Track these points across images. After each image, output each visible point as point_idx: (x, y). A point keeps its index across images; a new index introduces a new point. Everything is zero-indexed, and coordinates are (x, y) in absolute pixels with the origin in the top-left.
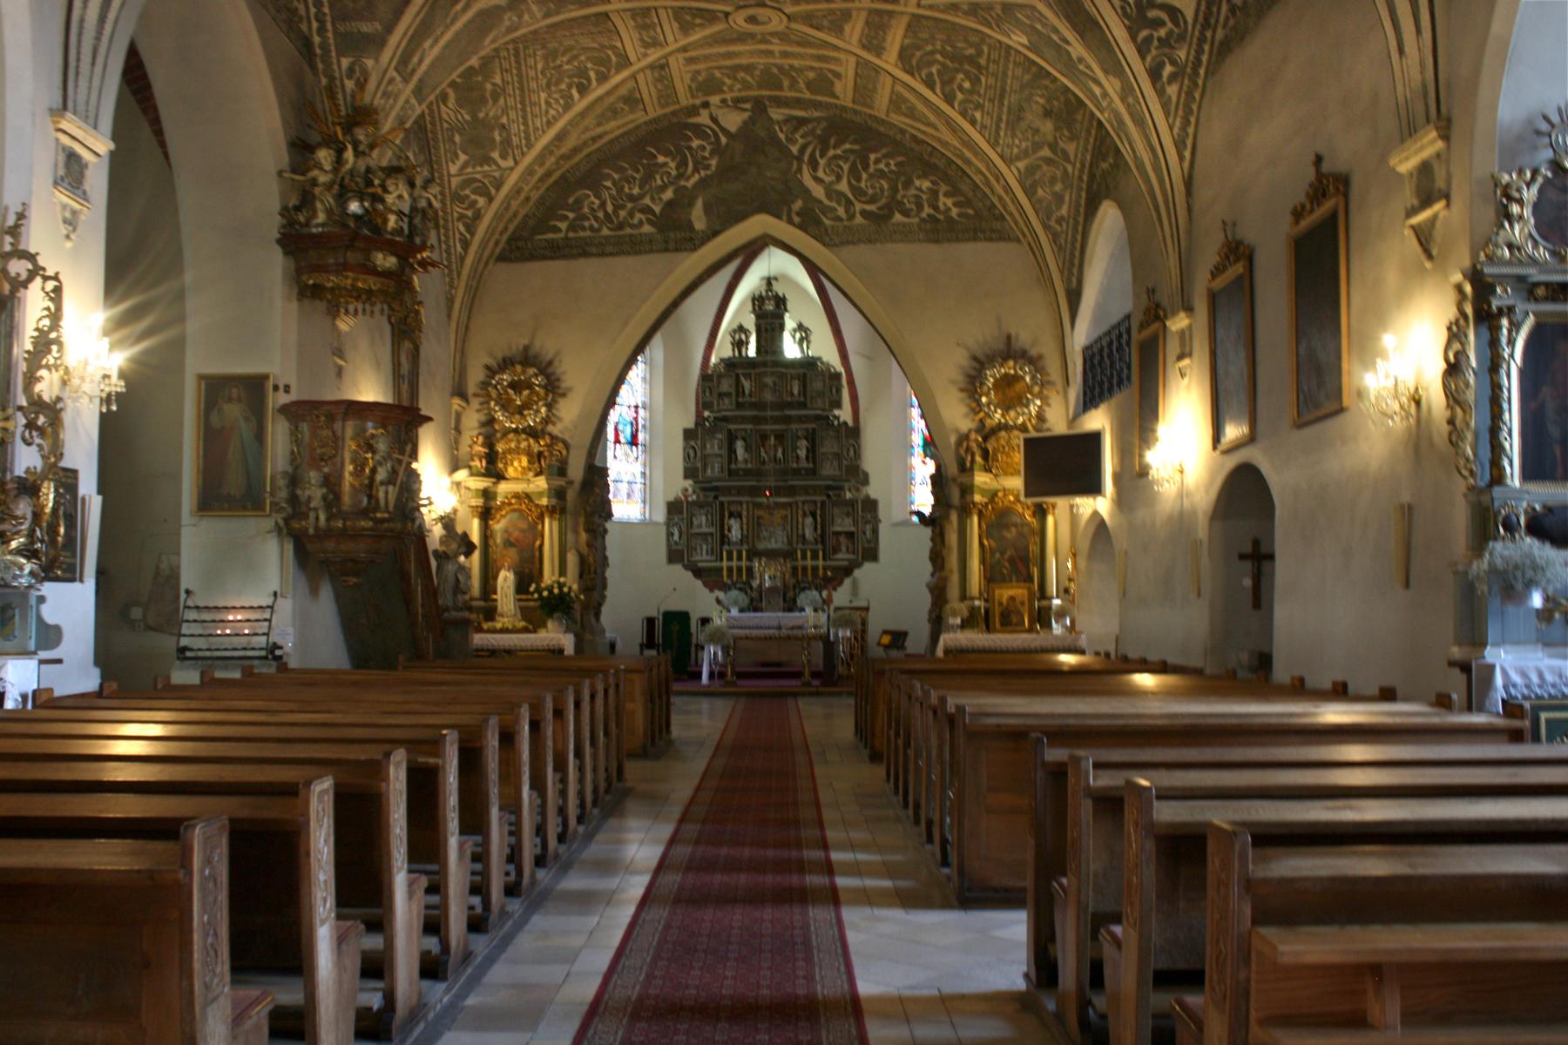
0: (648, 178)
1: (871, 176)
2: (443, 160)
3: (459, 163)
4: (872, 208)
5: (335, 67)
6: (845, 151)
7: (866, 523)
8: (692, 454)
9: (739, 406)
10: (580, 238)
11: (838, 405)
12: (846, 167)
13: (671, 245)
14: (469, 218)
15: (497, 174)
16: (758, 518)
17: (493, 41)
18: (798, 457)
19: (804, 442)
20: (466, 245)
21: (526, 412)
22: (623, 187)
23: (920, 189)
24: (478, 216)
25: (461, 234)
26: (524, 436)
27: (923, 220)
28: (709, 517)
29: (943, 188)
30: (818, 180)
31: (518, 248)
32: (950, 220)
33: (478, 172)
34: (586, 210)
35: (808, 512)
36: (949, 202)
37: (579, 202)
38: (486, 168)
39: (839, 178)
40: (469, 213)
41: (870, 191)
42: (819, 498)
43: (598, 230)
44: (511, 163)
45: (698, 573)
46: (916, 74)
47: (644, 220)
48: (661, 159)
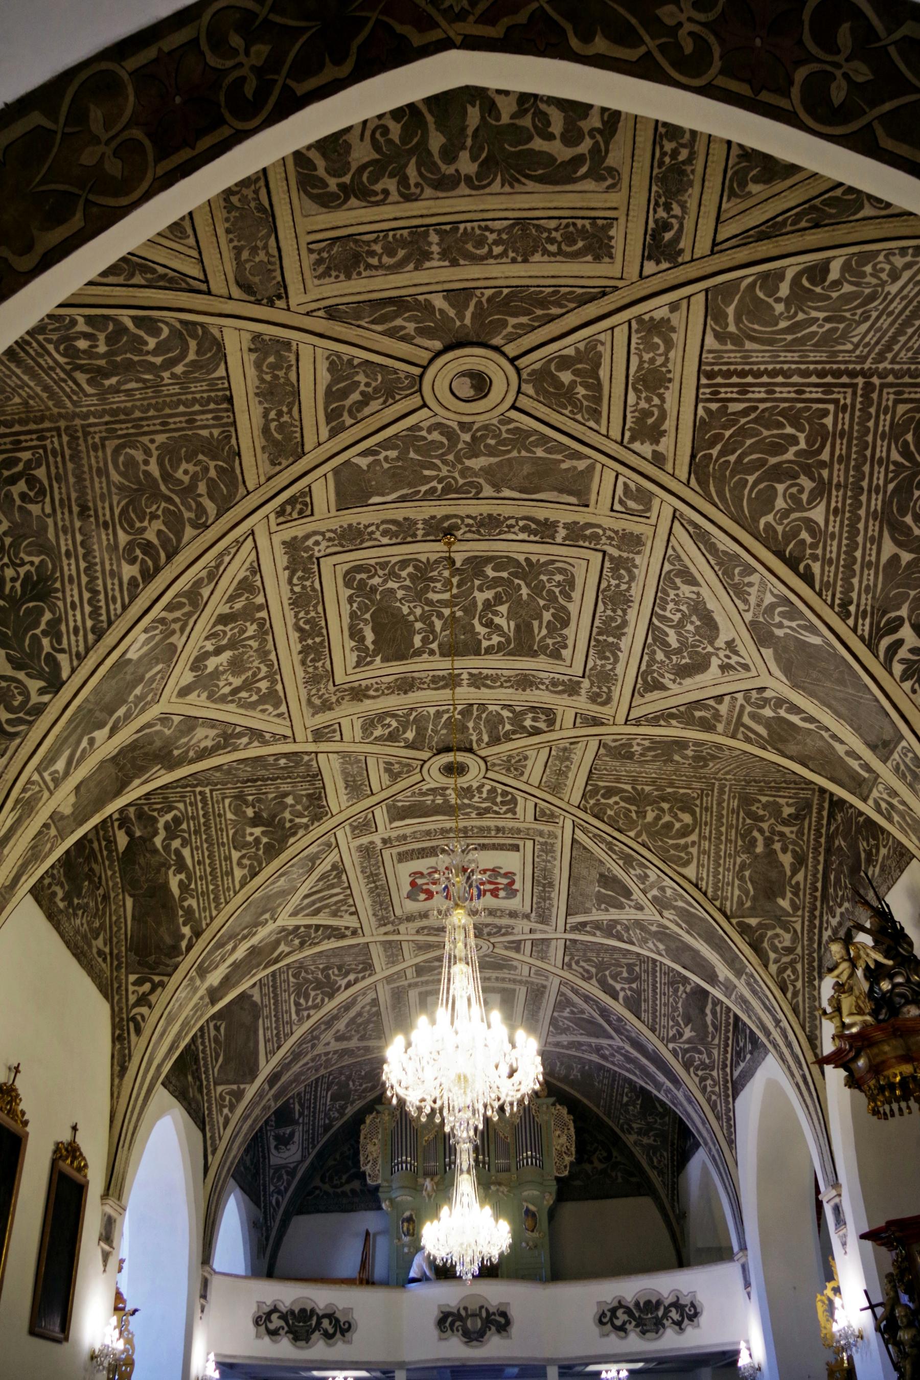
46: (178, 325)
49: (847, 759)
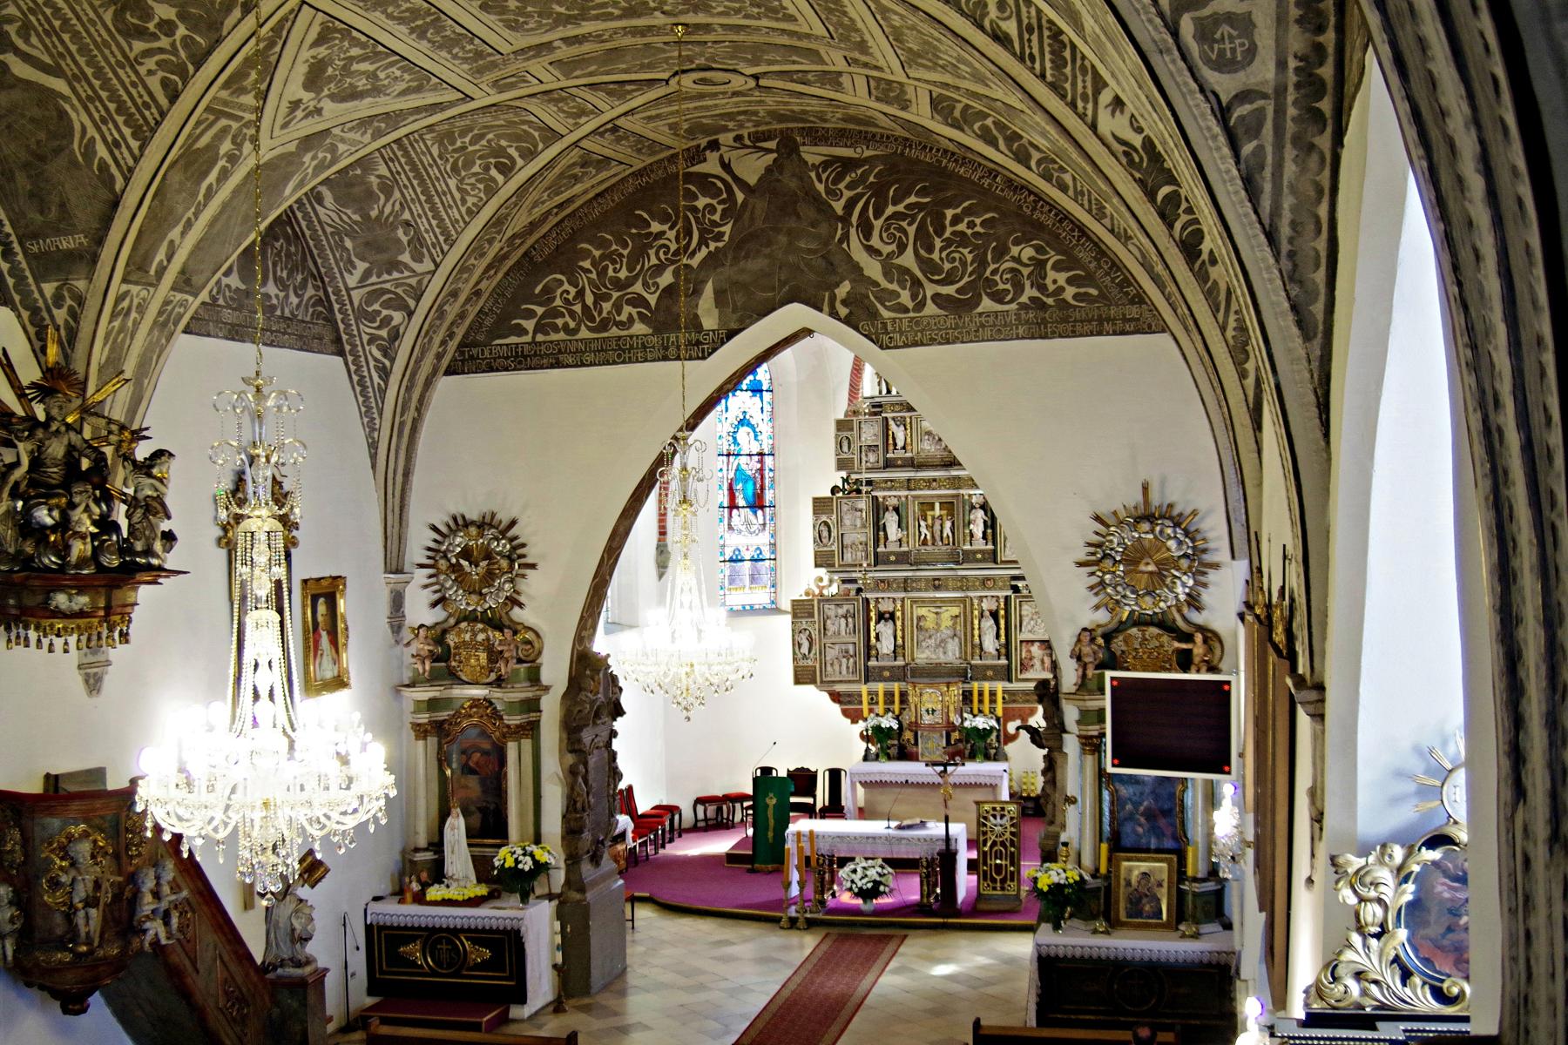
0: (639, 253)
1: (948, 243)
2: (336, 270)
3: (358, 274)
4: (949, 290)
5: (36, 295)
6: (907, 207)
8: (825, 534)
9: (889, 464)
10: (551, 342)
12: (912, 230)
13: (672, 351)
14: (383, 339)
15: (413, 281)
16: (919, 618)
17: (295, 190)
18: (972, 535)
20: (385, 373)
21: (484, 591)
22: (606, 267)
23: (1017, 260)
24: (395, 335)
25: (376, 360)
26: (480, 626)
27: (1023, 306)
28: (850, 620)
29: (1053, 257)
30: (872, 251)
31: (472, 357)
32: (1063, 304)
33: (388, 280)
34: (558, 302)
35: (987, 613)
36: (1062, 278)
37: (548, 290)
38: (396, 275)
39: (902, 248)
40: (384, 333)
41: (947, 266)
43: (576, 331)
44: (427, 265)
45: (836, 697)
46: (966, 128)
47: (635, 316)
48: (656, 227)
49: (165, 244)
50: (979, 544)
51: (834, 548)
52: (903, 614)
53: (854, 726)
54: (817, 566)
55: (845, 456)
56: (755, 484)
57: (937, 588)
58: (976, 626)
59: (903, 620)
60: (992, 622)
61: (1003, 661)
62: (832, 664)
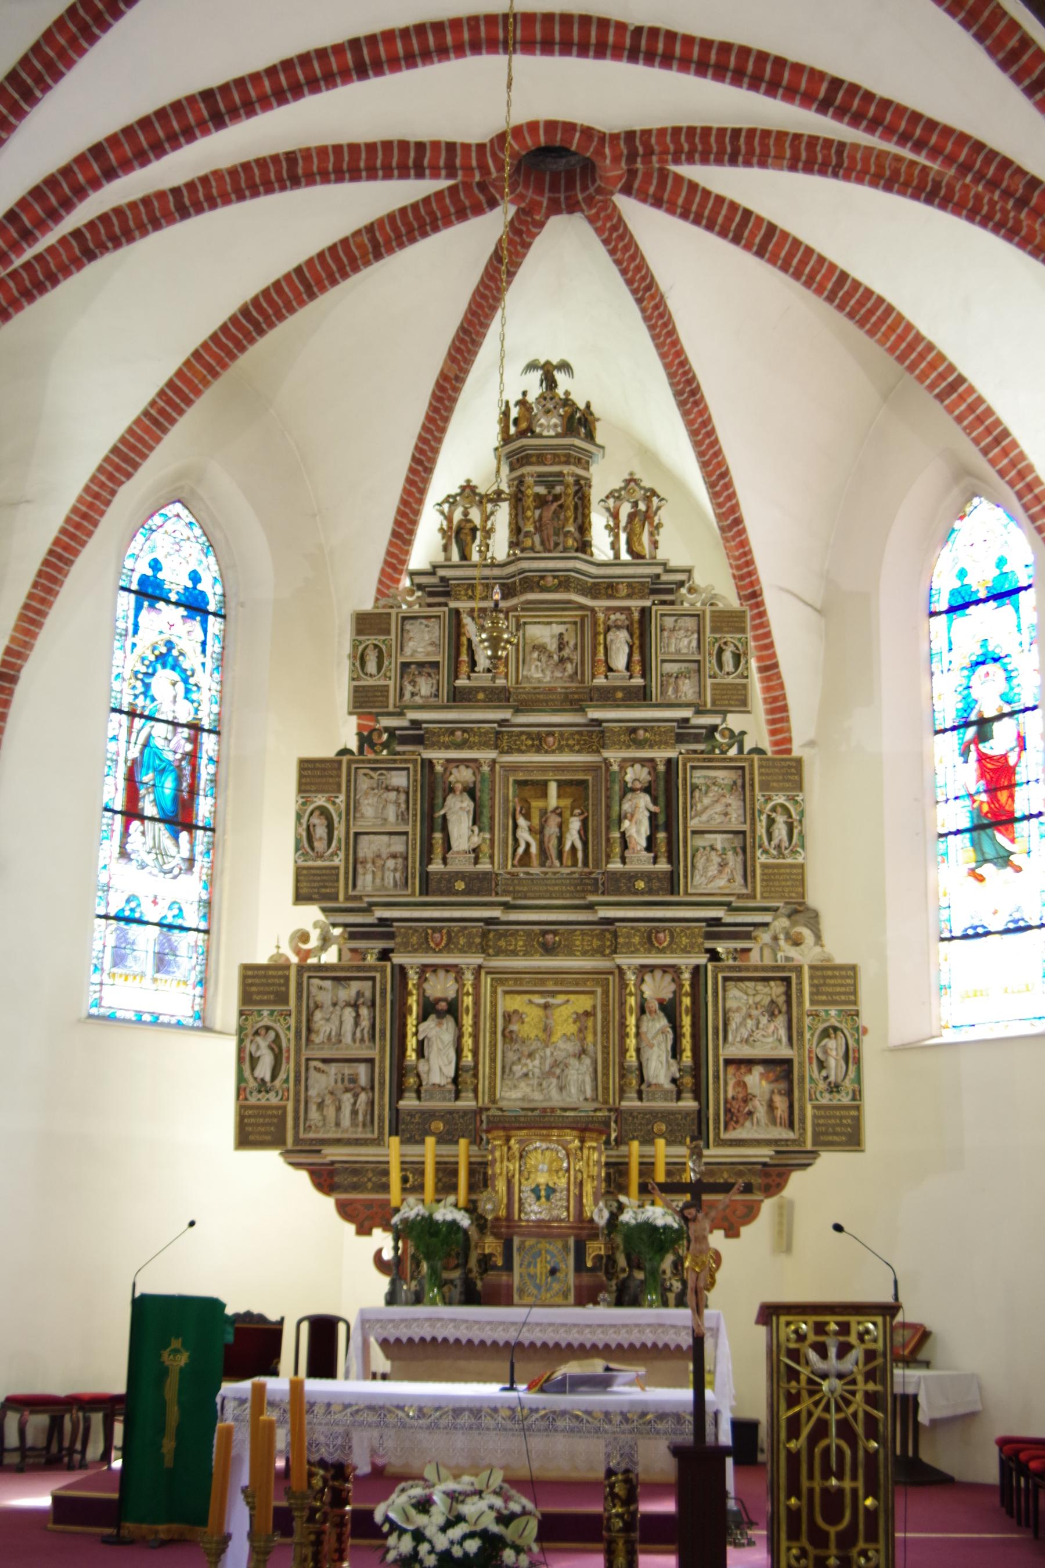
7: (825, 1034)
8: (321, 832)
9: (459, 697)
11: (740, 701)
16: (508, 1017)
19: (644, 801)
28: (364, 1012)
35: (655, 1005)
42: (686, 961)
50: (640, 861)
51: (338, 861)
52: (476, 1003)
53: (364, 1239)
54: (301, 897)
55: (370, 682)
56: (179, 779)
57: (549, 950)
58: (632, 1030)
59: (476, 1017)
60: (663, 1022)
61: (689, 1103)
62: (321, 1106)
